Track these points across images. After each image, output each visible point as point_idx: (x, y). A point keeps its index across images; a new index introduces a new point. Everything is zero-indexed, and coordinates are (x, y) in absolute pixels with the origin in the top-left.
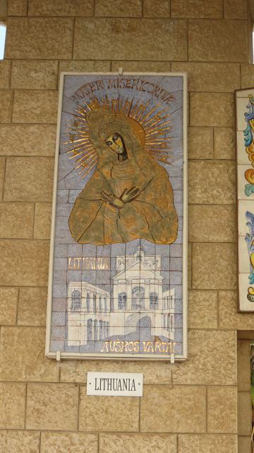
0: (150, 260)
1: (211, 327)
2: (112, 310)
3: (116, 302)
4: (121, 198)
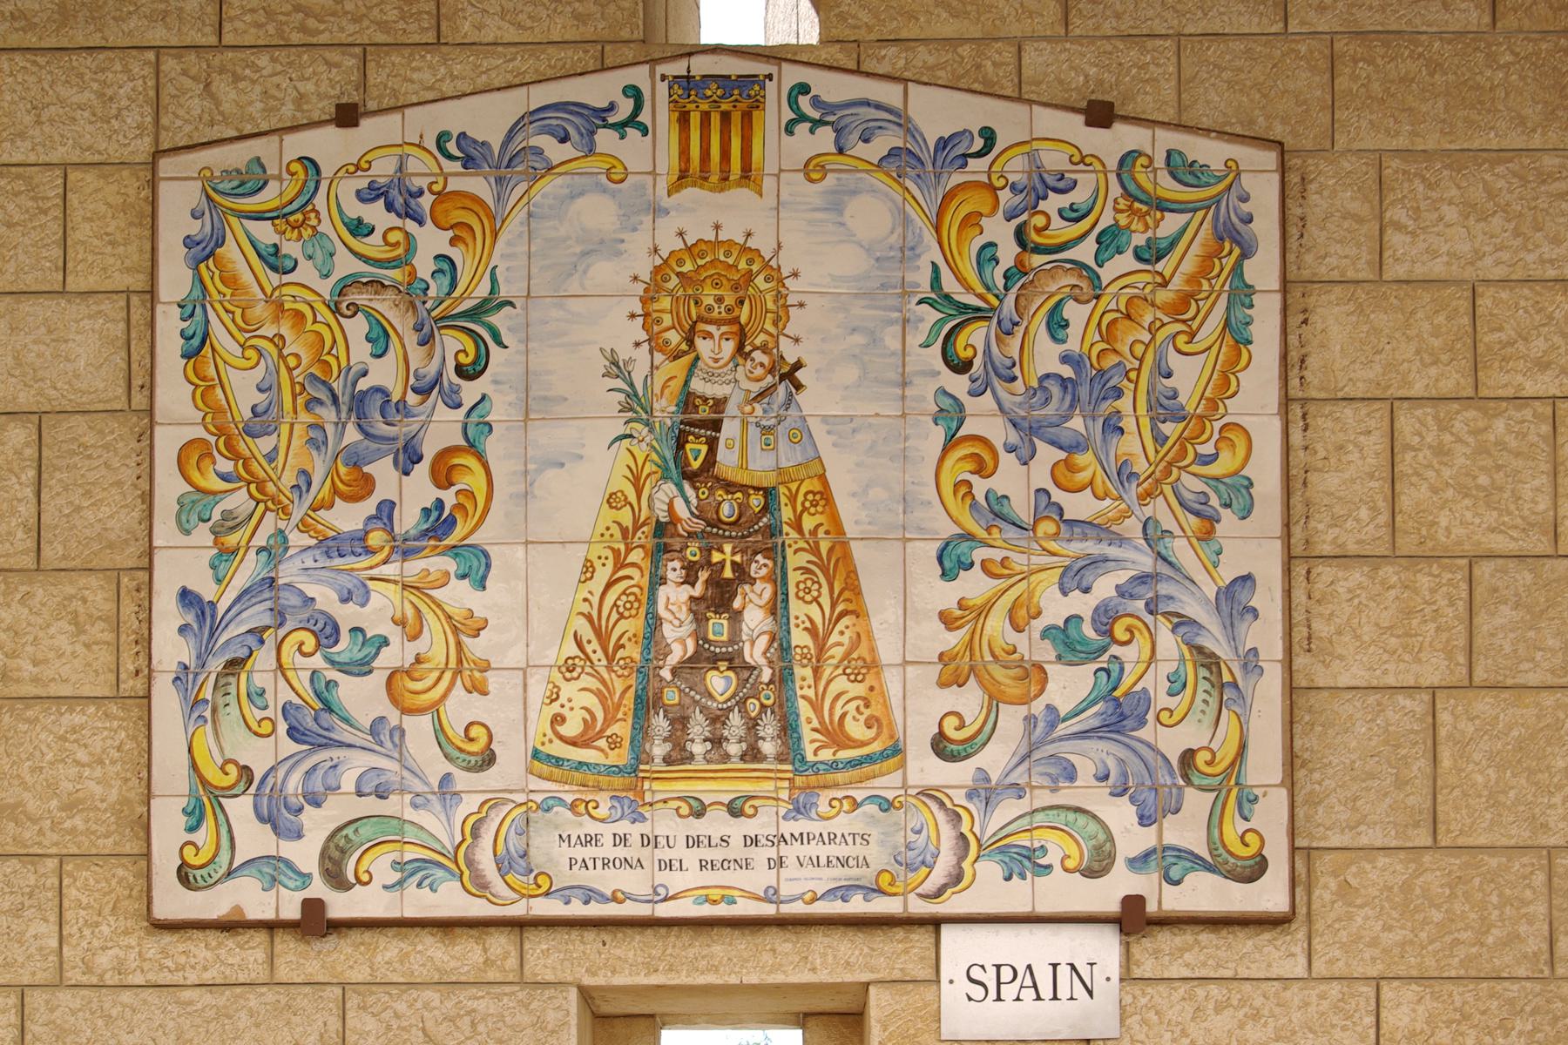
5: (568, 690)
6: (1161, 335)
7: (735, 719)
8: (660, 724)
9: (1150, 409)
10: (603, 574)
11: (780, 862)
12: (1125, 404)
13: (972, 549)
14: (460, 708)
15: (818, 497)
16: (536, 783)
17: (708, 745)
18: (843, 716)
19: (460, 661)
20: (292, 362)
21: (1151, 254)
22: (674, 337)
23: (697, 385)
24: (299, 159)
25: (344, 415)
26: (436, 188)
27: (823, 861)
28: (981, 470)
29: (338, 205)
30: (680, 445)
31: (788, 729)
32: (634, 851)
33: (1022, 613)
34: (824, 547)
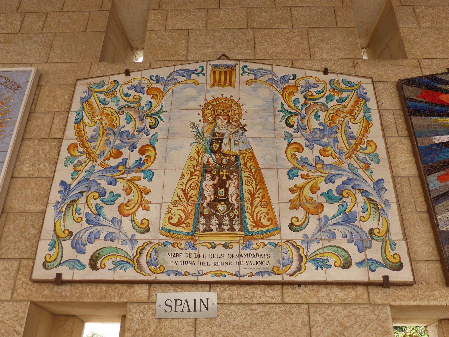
5: (174, 209)
6: (346, 119)
7: (226, 218)
8: (202, 220)
9: (346, 136)
10: (187, 178)
11: (241, 263)
12: (339, 135)
13: (298, 171)
14: (140, 215)
15: (251, 158)
16: (162, 237)
17: (218, 226)
18: (260, 218)
19: (141, 201)
20: (104, 125)
21: (341, 101)
22: (210, 119)
23: (216, 130)
25: (116, 137)
26: (148, 86)
27: (255, 263)
28: (299, 151)
30: (211, 144)
31: (243, 224)
32: (191, 259)
33: (314, 189)
34: (253, 171)
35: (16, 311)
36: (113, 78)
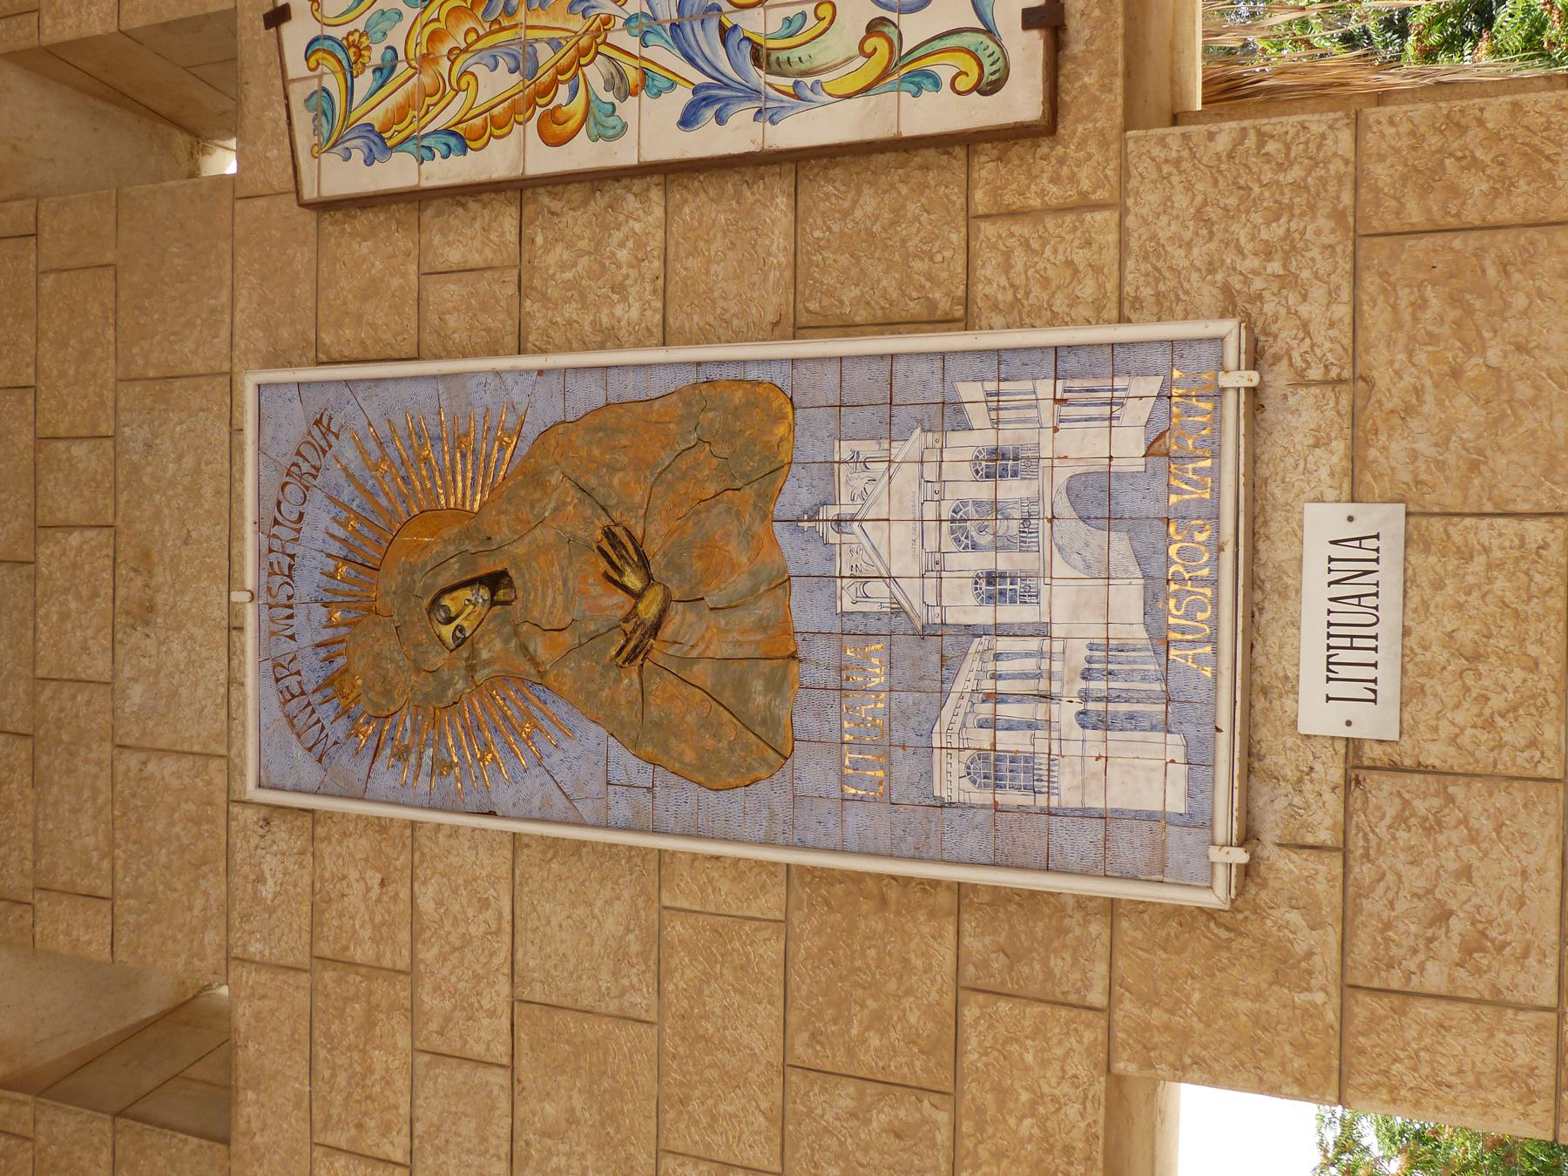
0: (851, 481)
1: (1112, 238)
2: (1042, 631)
3: (1009, 614)
4: (638, 596)
20: (472, 37)
24: (307, 59)
29: (343, 14)
35: (1160, 170)
36: (296, 65)
